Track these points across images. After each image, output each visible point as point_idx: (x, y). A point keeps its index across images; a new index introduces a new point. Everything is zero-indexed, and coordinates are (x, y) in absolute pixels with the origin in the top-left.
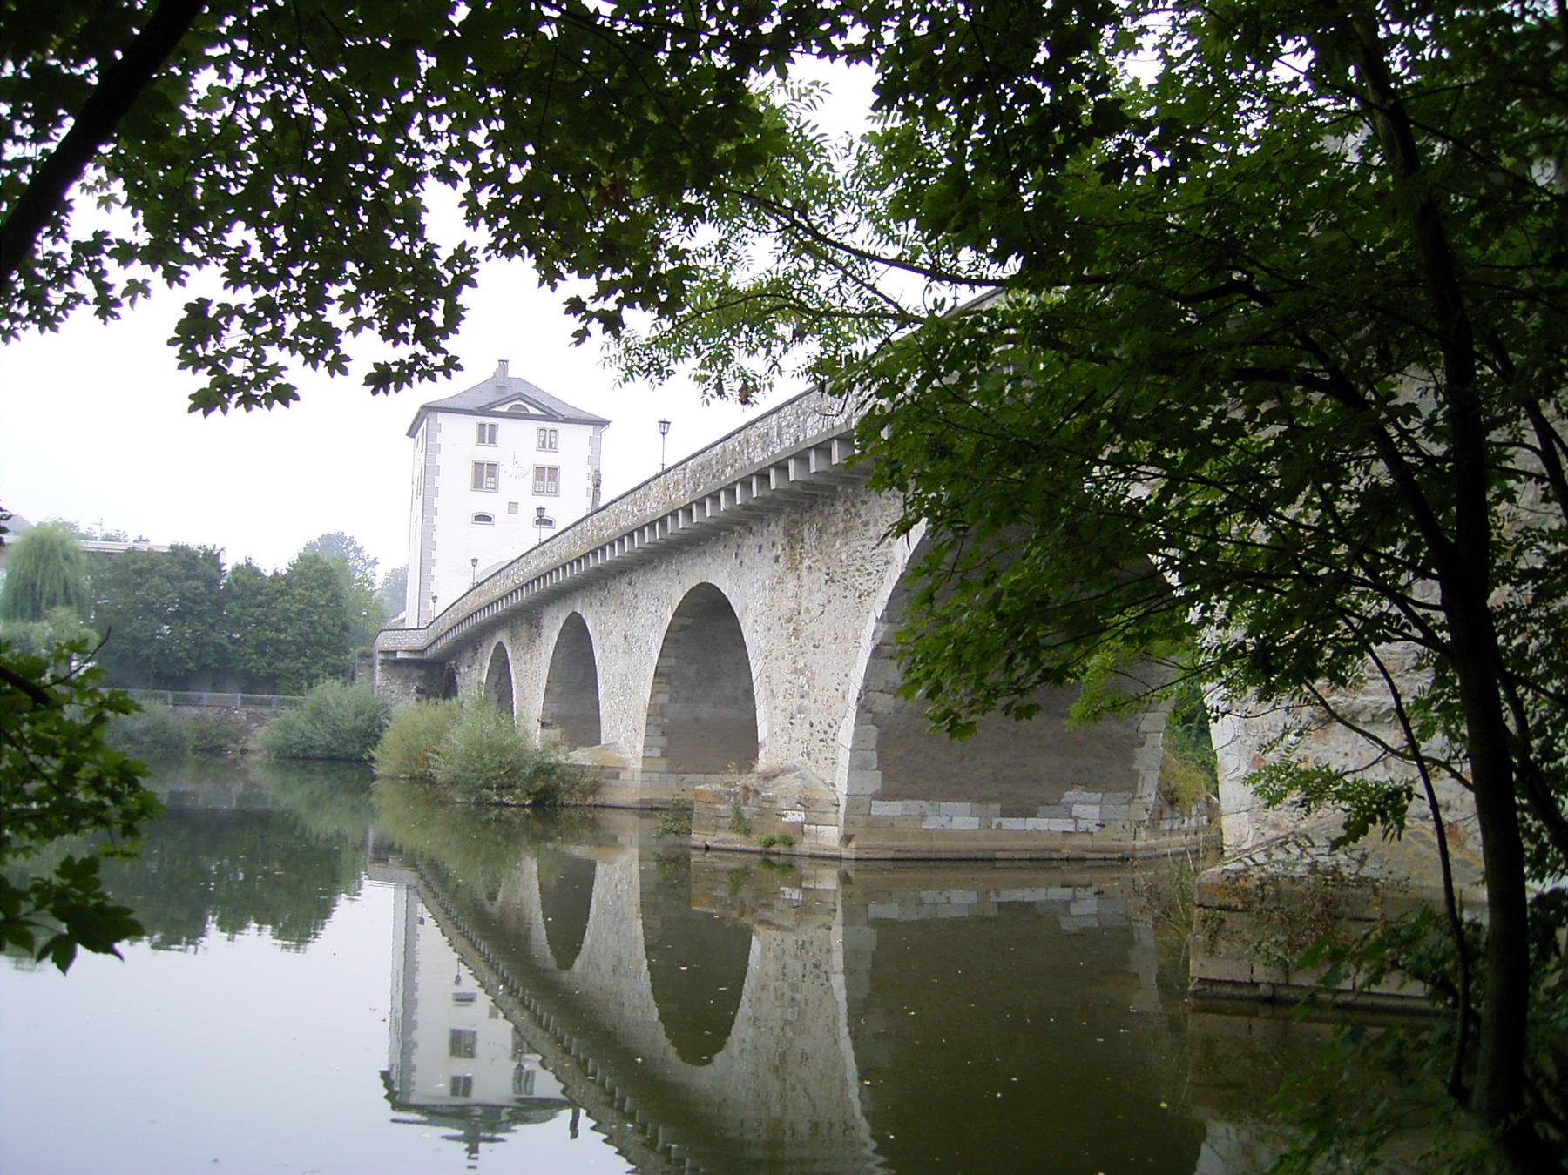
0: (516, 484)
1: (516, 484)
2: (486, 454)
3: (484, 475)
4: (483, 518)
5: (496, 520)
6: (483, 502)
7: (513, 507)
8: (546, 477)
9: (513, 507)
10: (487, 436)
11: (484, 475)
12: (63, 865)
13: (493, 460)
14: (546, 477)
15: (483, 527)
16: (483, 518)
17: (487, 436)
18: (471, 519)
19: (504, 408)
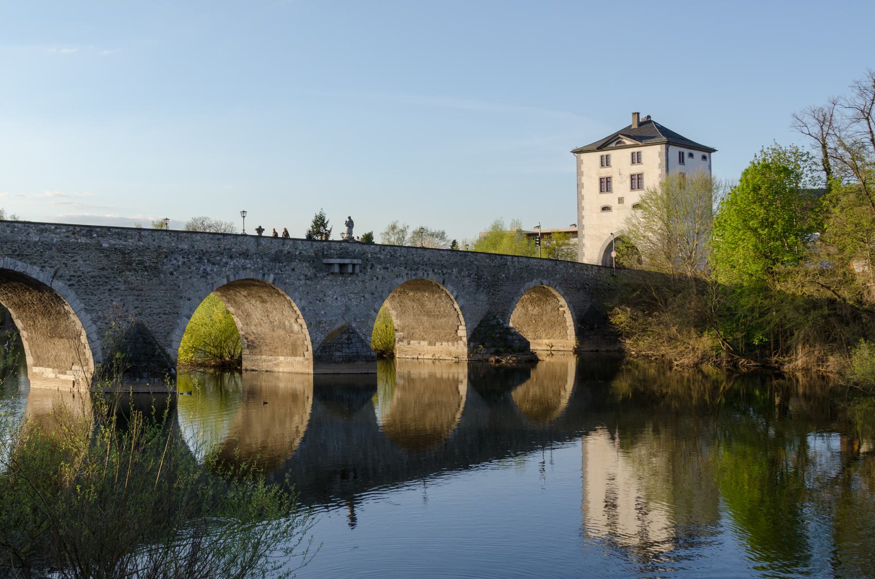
0: (621, 186)
1: (621, 186)
2: (605, 172)
3: (605, 185)
4: (605, 209)
5: (613, 209)
6: (607, 199)
7: (621, 200)
8: (636, 181)
9: (621, 200)
10: (605, 162)
11: (605, 185)
12: (392, 356)
13: (609, 175)
14: (636, 181)
15: (605, 213)
16: (605, 209)
17: (605, 162)
18: (600, 210)
19: (613, 145)
